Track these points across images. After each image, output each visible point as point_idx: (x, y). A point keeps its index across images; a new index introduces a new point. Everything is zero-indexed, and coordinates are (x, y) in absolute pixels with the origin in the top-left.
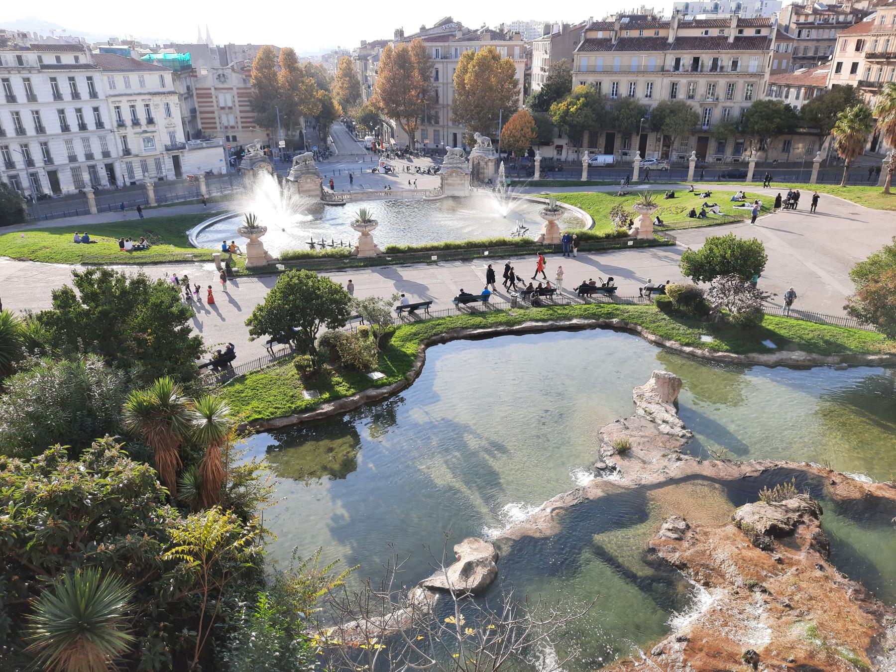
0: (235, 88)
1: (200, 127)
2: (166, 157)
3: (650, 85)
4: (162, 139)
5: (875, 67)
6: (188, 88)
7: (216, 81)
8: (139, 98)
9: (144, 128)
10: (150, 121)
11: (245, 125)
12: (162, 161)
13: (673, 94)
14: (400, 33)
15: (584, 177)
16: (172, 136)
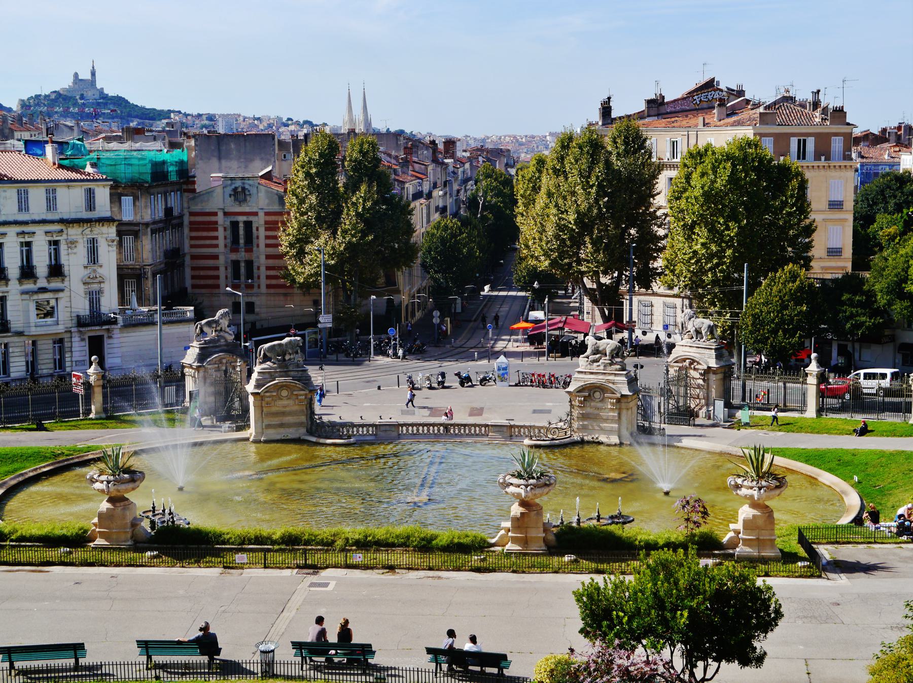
0: (261, 214)
1: (188, 283)
2: (76, 338)
4: (73, 301)
6: (168, 211)
7: (230, 201)
8: (39, 230)
9: (42, 283)
10: (56, 270)
11: (274, 282)
12: (67, 345)
14: (606, 110)
16: (94, 298)
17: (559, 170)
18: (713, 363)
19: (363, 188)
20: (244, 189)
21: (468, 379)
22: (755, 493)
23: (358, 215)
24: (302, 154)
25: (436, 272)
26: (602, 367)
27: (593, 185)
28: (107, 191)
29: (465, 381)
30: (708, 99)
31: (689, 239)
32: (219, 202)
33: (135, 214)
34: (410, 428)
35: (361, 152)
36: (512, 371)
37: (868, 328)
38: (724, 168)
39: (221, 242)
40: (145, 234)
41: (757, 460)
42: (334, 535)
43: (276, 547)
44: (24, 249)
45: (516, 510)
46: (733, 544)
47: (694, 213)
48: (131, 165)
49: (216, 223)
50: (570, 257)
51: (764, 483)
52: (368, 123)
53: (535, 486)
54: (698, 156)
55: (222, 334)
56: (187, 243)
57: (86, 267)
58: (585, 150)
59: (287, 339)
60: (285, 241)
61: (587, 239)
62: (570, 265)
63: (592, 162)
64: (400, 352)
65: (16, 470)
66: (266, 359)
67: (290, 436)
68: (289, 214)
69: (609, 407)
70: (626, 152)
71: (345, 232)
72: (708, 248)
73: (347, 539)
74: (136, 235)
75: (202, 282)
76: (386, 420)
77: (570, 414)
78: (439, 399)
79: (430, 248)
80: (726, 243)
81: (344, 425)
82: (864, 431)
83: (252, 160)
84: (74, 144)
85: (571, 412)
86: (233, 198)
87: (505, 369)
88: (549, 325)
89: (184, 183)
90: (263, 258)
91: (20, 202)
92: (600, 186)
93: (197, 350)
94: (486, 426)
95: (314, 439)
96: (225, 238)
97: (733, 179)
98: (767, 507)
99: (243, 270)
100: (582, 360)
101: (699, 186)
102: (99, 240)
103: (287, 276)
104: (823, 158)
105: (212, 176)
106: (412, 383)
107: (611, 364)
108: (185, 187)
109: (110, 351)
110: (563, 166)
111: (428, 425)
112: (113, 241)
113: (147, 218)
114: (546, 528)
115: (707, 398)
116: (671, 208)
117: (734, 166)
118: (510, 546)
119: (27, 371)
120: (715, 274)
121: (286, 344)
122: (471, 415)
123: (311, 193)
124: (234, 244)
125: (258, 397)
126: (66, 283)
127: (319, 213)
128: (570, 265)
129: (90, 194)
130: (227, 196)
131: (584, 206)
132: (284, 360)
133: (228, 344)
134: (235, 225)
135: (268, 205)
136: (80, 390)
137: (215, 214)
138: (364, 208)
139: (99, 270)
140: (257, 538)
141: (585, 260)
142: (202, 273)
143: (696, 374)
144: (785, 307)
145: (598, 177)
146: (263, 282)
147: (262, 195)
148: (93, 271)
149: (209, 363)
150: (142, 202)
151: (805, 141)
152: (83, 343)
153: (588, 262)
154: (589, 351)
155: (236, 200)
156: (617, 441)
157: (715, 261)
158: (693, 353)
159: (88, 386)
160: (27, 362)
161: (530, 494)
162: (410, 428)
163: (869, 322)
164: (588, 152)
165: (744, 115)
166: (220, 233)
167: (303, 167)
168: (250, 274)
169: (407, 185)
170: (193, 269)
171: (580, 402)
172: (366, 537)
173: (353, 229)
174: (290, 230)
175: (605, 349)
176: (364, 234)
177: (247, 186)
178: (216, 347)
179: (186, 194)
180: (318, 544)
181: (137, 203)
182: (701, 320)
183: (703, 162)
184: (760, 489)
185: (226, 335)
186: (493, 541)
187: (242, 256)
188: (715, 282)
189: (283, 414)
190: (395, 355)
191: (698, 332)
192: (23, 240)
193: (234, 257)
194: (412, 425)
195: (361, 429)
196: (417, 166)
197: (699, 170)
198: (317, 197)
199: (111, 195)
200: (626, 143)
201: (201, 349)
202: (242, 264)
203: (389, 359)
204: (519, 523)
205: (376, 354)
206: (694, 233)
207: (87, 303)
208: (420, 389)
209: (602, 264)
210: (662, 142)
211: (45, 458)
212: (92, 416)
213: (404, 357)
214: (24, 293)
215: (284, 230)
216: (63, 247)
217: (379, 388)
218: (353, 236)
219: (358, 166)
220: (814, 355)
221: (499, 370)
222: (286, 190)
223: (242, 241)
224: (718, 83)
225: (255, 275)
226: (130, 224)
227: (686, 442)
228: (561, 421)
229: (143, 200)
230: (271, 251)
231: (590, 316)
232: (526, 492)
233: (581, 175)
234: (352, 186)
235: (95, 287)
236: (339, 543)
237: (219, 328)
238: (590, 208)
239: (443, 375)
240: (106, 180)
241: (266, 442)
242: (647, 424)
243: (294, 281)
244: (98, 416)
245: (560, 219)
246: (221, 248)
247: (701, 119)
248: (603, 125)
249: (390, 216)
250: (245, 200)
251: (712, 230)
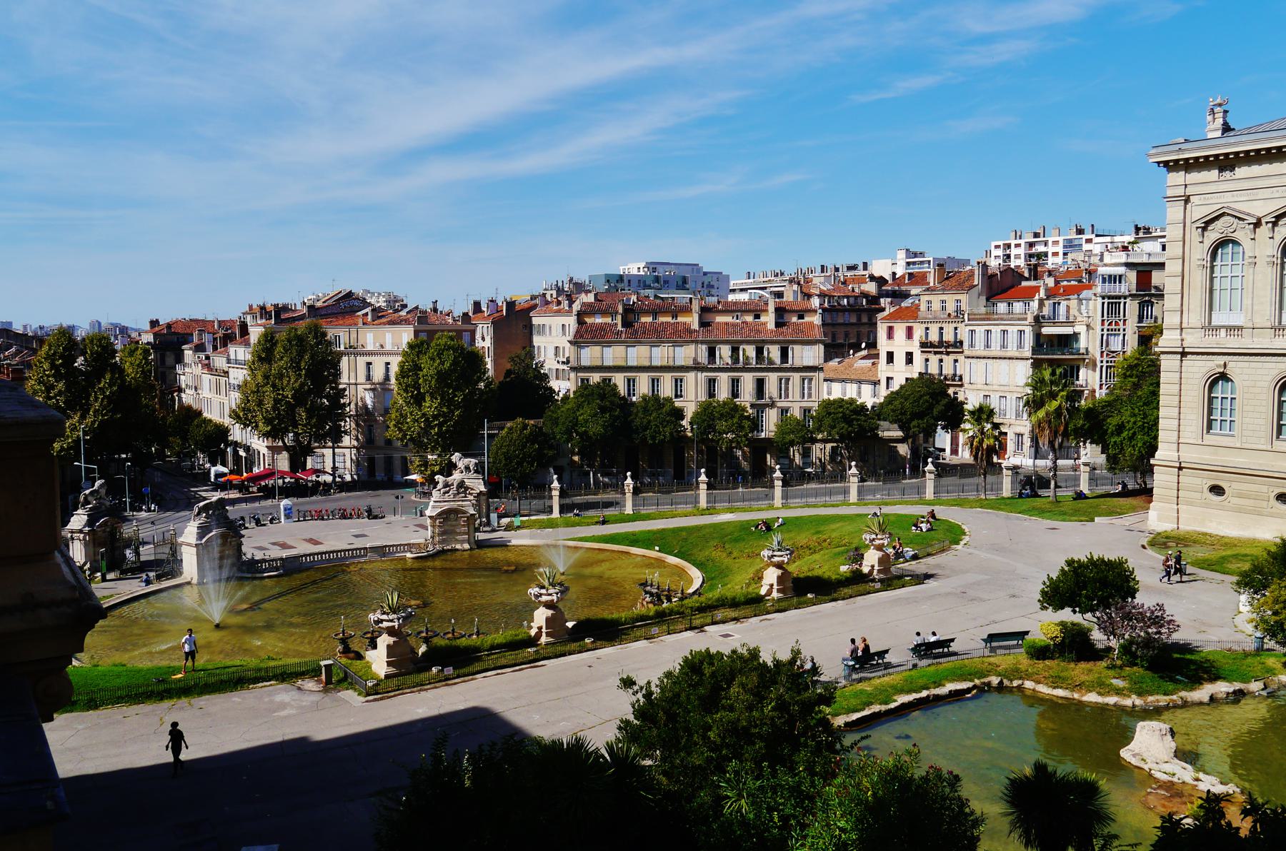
3: (678, 383)
5: (934, 359)
13: (711, 394)
15: (629, 510)
18: (483, 488)
19: (108, 376)
30: (347, 306)
35: (100, 346)
111: (313, 554)
144: (524, 446)
182: (467, 460)
188: (439, 434)
190: (149, 510)
191: (467, 468)
210: (340, 334)
227: (514, 542)
238: (302, 385)
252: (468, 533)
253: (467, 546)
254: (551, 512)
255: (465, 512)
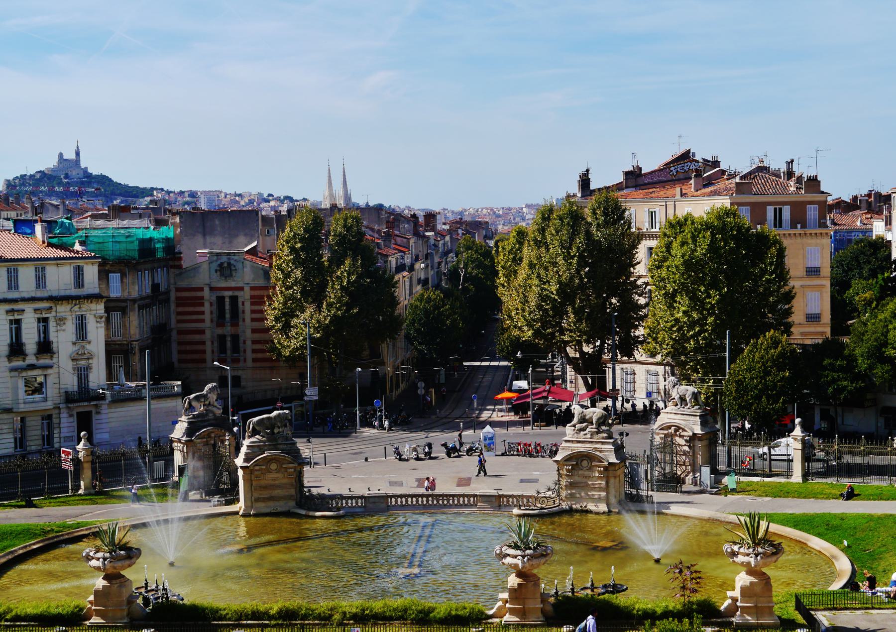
0: (247, 289)
1: (175, 357)
2: (64, 415)
6: (155, 287)
7: (216, 276)
8: (29, 308)
9: (31, 360)
10: (45, 347)
11: (260, 356)
12: (55, 421)
14: (585, 182)
16: (83, 374)
17: (540, 242)
18: (698, 430)
19: (348, 262)
20: (229, 264)
21: (454, 449)
22: (752, 560)
23: (343, 288)
24: (288, 229)
25: (420, 344)
26: (589, 436)
27: (575, 255)
28: (96, 268)
29: (451, 451)
30: (684, 170)
31: (671, 307)
32: (205, 277)
33: (123, 290)
34: (399, 499)
35: (345, 226)
36: (498, 441)
37: (850, 392)
38: (704, 237)
39: (207, 317)
40: (133, 310)
41: (753, 526)
42: (331, 609)
43: (273, 622)
44: (14, 326)
45: (513, 581)
46: (733, 609)
47: (675, 282)
48: (119, 242)
49: (202, 298)
50: (553, 327)
51: (760, 550)
52: (347, 198)
53: (532, 557)
54: (677, 226)
55: (210, 408)
56: (173, 318)
57: (74, 344)
58: (566, 221)
59: (275, 413)
60: (270, 316)
61: (570, 309)
62: (553, 334)
63: (573, 233)
64: (386, 424)
65: (5, 548)
66: (255, 432)
67: (280, 510)
68: (274, 288)
69: (597, 475)
70: (606, 223)
71: (330, 305)
72: (689, 316)
73: (344, 613)
74: (124, 311)
75: (189, 357)
76: (374, 492)
77: (558, 483)
78: (427, 469)
79: (413, 319)
80: (708, 310)
81: (333, 497)
82: (850, 495)
83: (237, 236)
84: (62, 223)
85: (559, 481)
86: (219, 273)
87: (491, 439)
88: (534, 395)
89: (171, 259)
90: (248, 332)
91: (9, 281)
92: (581, 257)
93: (186, 425)
94: (475, 496)
95: (303, 512)
96: (212, 313)
97: (713, 248)
98: (765, 574)
99: (229, 344)
100: (569, 429)
101: (679, 255)
102: (88, 316)
103: (273, 349)
104: (799, 226)
105: (199, 252)
106: (399, 454)
107: (598, 433)
108: (171, 263)
109: (98, 426)
110: (544, 237)
112: (101, 318)
113: (135, 294)
114: (544, 597)
115: (693, 464)
116: (652, 277)
117: (713, 235)
118: (508, 618)
119: (16, 448)
120: (697, 342)
121: (275, 417)
122: (458, 485)
123: (296, 268)
124: (220, 319)
125: (248, 471)
126: (55, 360)
127: (304, 287)
128: (553, 334)
129: (79, 273)
130: (213, 272)
131: (565, 277)
132: (273, 433)
133: (216, 418)
134: (220, 300)
135: (254, 279)
136: (69, 466)
137: (202, 289)
138: (348, 282)
139: (88, 347)
140: (253, 613)
141: (568, 330)
142: (188, 348)
143: (681, 441)
144: (768, 373)
145: (578, 248)
146: (250, 355)
147: (247, 270)
148: (82, 346)
149: (198, 437)
150: (129, 279)
151: (780, 209)
152: (71, 419)
153: (571, 331)
154: (575, 420)
155: (222, 275)
156: (606, 509)
157: (697, 329)
158: (678, 420)
159: (77, 462)
160: (15, 439)
161: (527, 565)
162: (399, 499)
163: (851, 386)
164: (568, 224)
165: (720, 185)
166: (207, 308)
167: (288, 242)
168: (236, 348)
169: (390, 259)
170: (180, 343)
171: (568, 470)
172: (363, 610)
173: (337, 303)
174: (276, 304)
175: (591, 418)
176: (349, 306)
177: (232, 262)
178: (205, 421)
179: (172, 270)
180: (315, 618)
181: (125, 280)
182: (684, 387)
183: (684, 231)
184: (757, 555)
185: (215, 409)
186: (491, 612)
187: (228, 330)
188: (697, 350)
189: (273, 487)
190: (382, 427)
191: (682, 399)
192: (12, 318)
193: (220, 331)
194: (401, 496)
195: (350, 501)
196: (399, 239)
197: (679, 239)
198: (302, 271)
199: (99, 272)
200: (605, 214)
201: (189, 423)
202: (229, 339)
203: (375, 431)
204: (516, 594)
205: (362, 426)
206: (676, 302)
207: (76, 379)
208: (407, 460)
209: (585, 333)
210: (641, 213)
211: (35, 535)
212: (81, 492)
213: (390, 429)
214: (13, 370)
215: (270, 305)
216: (52, 324)
217: (366, 460)
218: (338, 309)
219: (342, 240)
220: (797, 421)
221: (485, 439)
222: (271, 266)
223: (228, 316)
224: (694, 154)
225: (242, 349)
226: (117, 300)
227: (674, 509)
228: (549, 490)
229: (131, 278)
230: (257, 325)
231: (573, 385)
232: (523, 562)
233: (562, 246)
234: (337, 261)
235: (83, 363)
236: (337, 617)
237: (207, 402)
238: (572, 278)
239: (430, 445)
240: (95, 257)
241: (255, 515)
242: (634, 492)
243: (280, 354)
244: (87, 492)
245: (542, 289)
246: (208, 323)
247: (678, 189)
248: (582, 197)
249: (374, 289)
250: (231, 275)
251: (693, 298)
252: (607, 489)
253: (603, 508)
254: (788, 474)
255: (600, 460)
